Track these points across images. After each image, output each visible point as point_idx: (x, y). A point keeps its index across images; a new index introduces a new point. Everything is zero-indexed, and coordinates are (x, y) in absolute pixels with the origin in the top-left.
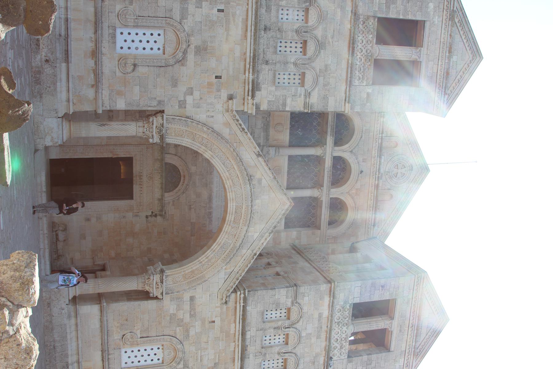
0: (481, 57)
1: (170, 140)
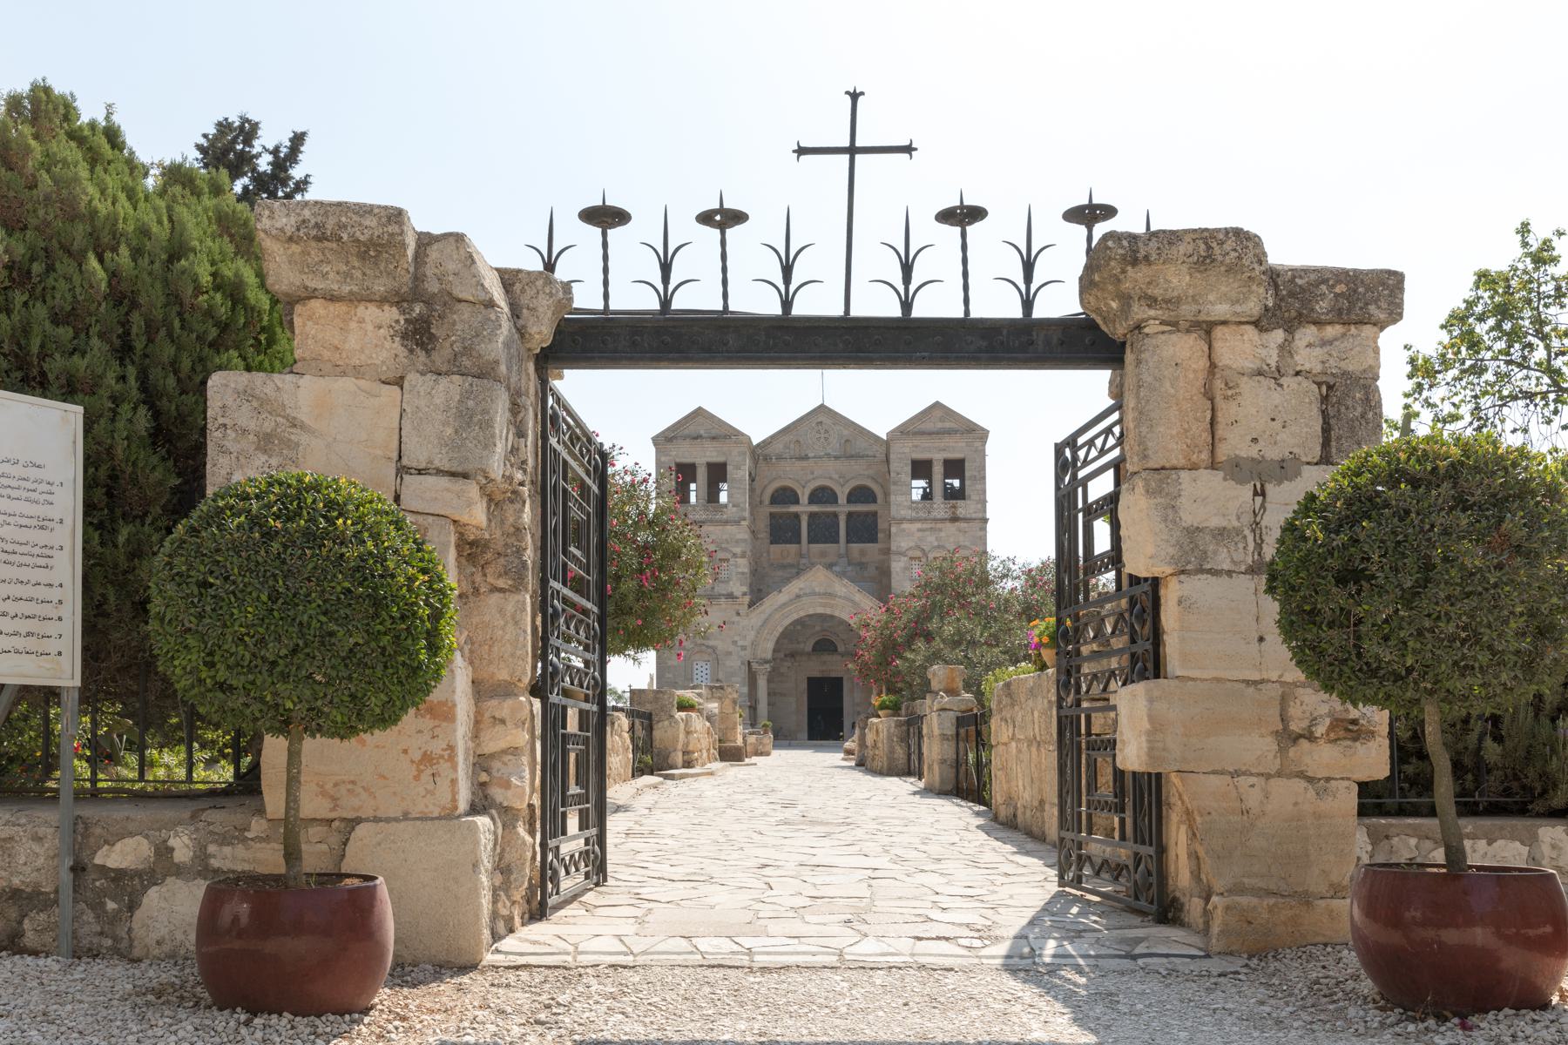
1: (769, 656)
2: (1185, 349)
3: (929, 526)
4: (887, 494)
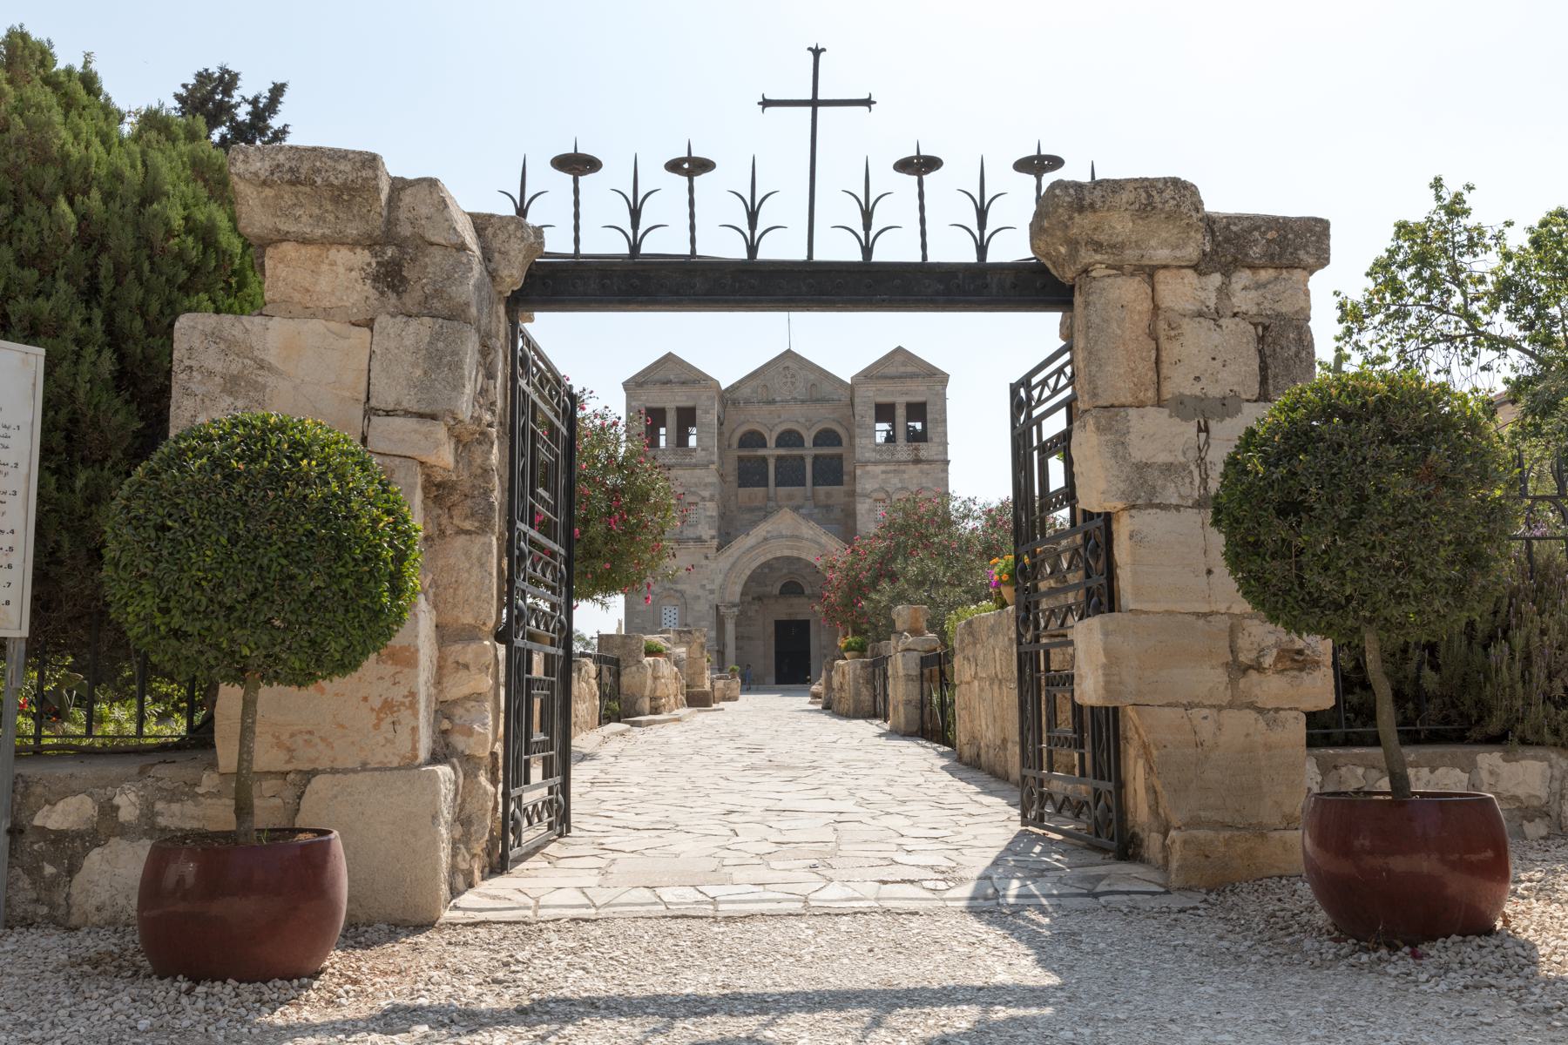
0: (670, 354)
1: (737, 599)
2: (1130, 290)
3: (891, 468)
4: (852, 437)
